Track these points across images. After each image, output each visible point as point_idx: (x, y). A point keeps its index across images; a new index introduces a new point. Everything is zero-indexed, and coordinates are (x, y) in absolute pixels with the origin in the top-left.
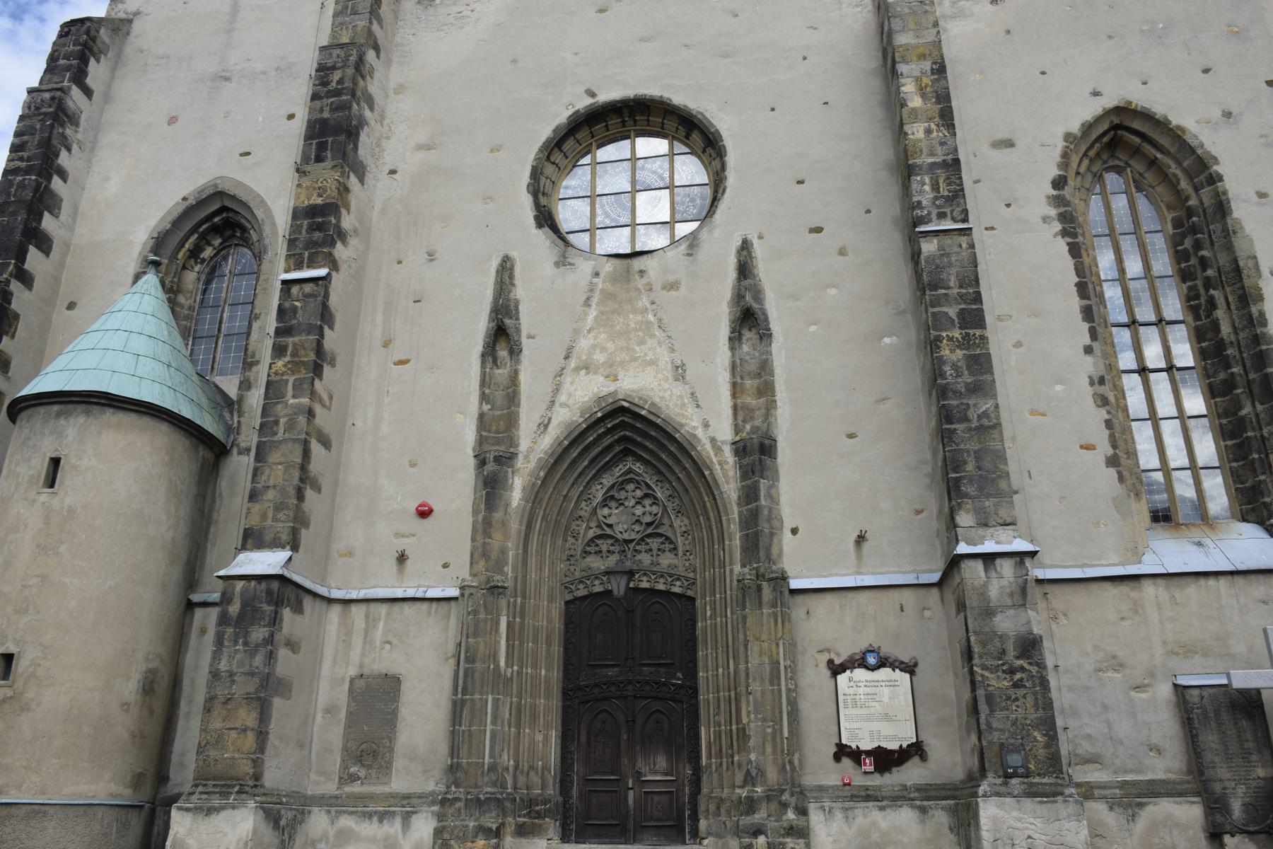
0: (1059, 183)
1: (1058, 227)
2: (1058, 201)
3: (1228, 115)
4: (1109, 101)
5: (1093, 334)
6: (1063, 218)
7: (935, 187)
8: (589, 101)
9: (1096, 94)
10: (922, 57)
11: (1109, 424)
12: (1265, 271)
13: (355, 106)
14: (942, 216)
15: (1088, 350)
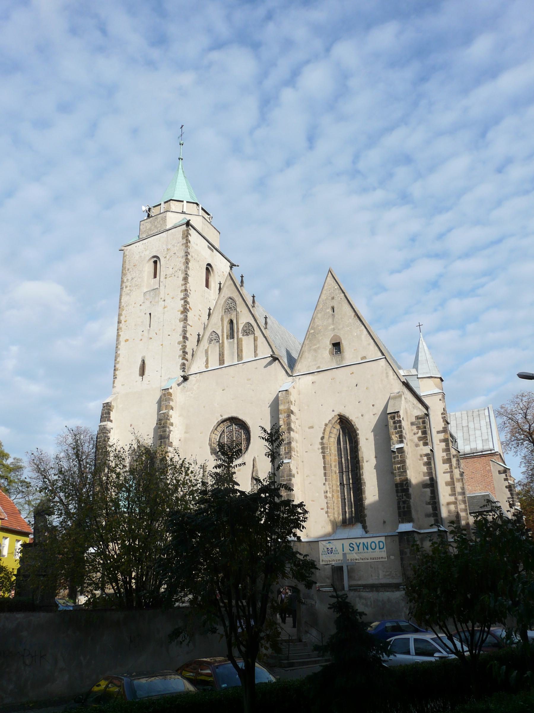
0: (322, 438)
1: (321, 451)
2: (322, 444)
3: (362, 415)
4: (336, 413)
5: (326, 480)
6: (323, 448)
7: (285, 450)
8: (221, 418)
9: (333, 411)
10: (285, 412)
11: (327, 503)
12: (365, 461)
13: (167, 429)
14: (286, 457)
15: (324, 484)
